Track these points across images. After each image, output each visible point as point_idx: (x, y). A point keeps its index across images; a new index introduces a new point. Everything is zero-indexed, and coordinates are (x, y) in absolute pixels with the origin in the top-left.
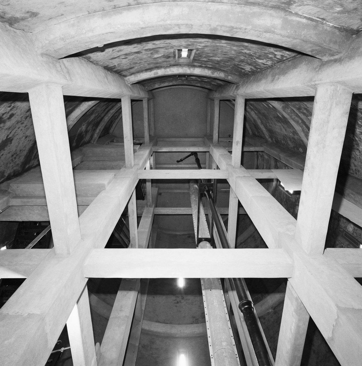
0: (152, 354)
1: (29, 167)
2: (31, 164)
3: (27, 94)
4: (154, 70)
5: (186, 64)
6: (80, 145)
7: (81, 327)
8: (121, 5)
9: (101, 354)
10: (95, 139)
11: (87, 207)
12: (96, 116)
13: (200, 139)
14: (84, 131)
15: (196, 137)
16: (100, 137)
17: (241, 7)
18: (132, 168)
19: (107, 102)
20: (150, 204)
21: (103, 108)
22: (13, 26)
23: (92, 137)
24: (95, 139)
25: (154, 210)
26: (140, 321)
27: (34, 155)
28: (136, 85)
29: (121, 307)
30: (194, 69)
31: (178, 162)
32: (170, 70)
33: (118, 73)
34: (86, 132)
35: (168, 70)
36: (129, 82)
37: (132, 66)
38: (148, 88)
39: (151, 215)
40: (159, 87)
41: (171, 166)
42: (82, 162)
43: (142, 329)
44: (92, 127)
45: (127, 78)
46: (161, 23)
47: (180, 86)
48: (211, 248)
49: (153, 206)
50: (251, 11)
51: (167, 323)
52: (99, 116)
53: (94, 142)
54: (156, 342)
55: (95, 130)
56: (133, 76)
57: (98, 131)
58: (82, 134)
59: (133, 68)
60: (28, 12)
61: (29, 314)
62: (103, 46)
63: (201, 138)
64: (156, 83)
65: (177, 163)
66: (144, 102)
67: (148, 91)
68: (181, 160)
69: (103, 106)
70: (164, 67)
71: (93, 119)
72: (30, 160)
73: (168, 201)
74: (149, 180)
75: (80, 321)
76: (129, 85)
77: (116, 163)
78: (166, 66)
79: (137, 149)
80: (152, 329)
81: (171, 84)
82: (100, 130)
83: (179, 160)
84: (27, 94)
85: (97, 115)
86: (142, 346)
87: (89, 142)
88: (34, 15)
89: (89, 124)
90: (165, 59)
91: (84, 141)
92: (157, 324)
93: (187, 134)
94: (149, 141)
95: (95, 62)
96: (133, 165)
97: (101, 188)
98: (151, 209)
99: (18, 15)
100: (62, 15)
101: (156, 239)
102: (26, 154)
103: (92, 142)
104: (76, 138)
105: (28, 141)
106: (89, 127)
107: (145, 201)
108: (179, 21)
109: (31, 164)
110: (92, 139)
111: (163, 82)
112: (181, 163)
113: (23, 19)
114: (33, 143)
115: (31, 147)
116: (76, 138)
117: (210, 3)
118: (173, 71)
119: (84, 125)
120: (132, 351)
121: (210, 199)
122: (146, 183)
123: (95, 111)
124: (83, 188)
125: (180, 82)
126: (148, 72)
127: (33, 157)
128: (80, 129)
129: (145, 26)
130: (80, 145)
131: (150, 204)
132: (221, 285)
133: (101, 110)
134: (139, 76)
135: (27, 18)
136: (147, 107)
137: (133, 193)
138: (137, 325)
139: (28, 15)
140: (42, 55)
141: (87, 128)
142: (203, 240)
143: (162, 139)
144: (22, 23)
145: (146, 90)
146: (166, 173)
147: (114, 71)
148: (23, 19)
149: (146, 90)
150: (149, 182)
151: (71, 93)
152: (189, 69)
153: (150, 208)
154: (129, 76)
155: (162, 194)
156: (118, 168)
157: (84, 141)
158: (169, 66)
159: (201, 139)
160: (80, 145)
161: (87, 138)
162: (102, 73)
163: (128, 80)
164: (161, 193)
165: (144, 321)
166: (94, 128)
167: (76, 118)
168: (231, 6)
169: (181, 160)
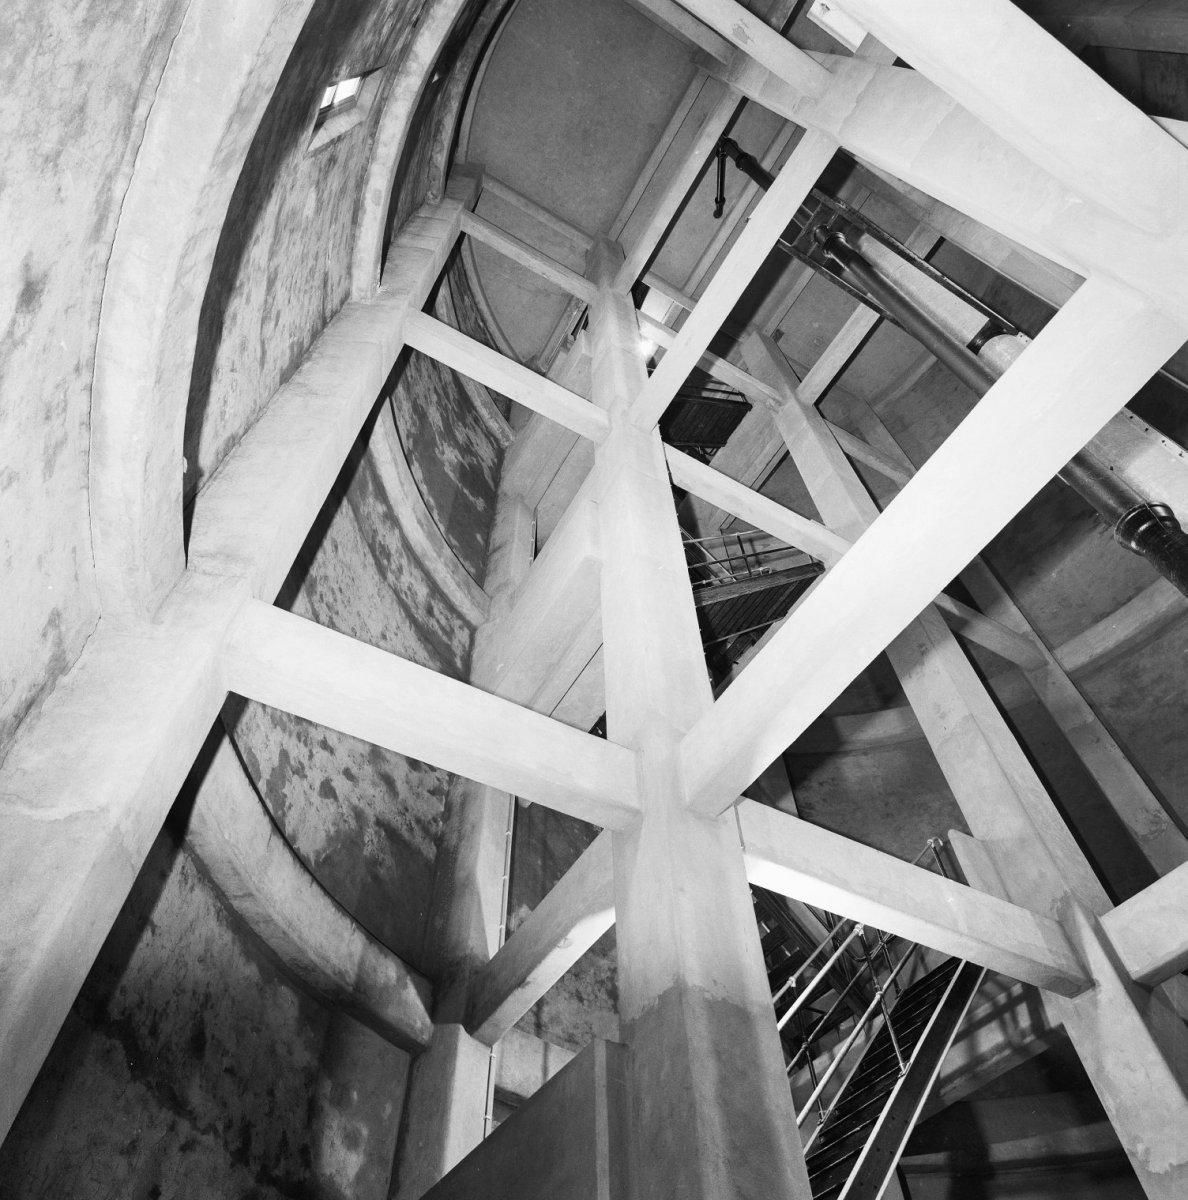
0: (1157, 700)
1: (462, 658)
2: (459, 651)
3: (232, 696)
4: (364, 198)
5: (388, 80)
6: (491, 484)
7: (831, 882)
8: (86, 409)
9: (982, 842)
10: (503, 432)
11: (601, 662)
12: (439, 403)
13: (695, 85)
14: (461, 459)
15: (683, 94)
16: (507, 419)
17: (175, 62)
18: (611, 429)
19: (388, 399)
20: (774, 399)
21: (423, 369)
22: (70, 665)
23: (489, 435)
24: (503, 432)
25: (798, 401)
26: (1046, 663)
27: (440, 632)
28: (393, 252)
29: (937, 707)
30: (416, 55)
31: (718, 213)
32: (386, 145)
33: (325, 324)
34: (467, 449)
35: (381, 151)
36: (369, 294)
37: (317, 282)
38: (435, 192)
39: (805, 423)
40: (445, 153)
41: (717, 246)
42: (535, 514)
43: (1069, 674)
44: (465, 425)
45: (355, 295)
46: (157, 332)
47: (483, 66)
48: (1021, 348)
49: (788, 392)
50: (197, 31)
51: (1130, 599)
52: (440, 391)
53: (508, 440)
54: (1141, 666)
55: (477, 419)
56: (355, 272)
57: (484, 412)
58: (464, 467)
59: (326, 274)
60: (44, 635)
61: (660, 997)
62: (186, 460)
63: (692, 79)
64: (431, 157)
65: (721, 220)
66: (468, 231)
67: (443, 198)
68: (720, 201)
69: (418, 370)
70: (368, 160)
71: (441, 415)
72: (448, 648)
73: (816, 325)
74: (703, 359)
75: (816, 876)
76: (379, 290)
77: (576, 458)
78: (367, 153)
79: (584, 351)
80: (1099, 650)
81: (455, 105)
82: (485, 404)
83: (714, 207)
84: (232, 696)
85: (434, 398)
86: (1112, 706)
87: (500, 453)
88: (55, 619)
89: (449, 434)
90: (336, 168)
91: (490, 468)
92: (1101, 626)
93: (652, 126)
94: (591, 287)
95: (252, 419)
96: (606, 422)
97: (592, 570)
98: (792, 406)
99: (46, 655)
100: (74, 550)
101: (891, 440)
102: (428, 652)
103: (506, 444)
104: (466, 491)
105: (396, 635)
106: (457, 434)
107: (757, 408)
108: (166, 280)
109: (459, 651)
110: (496, 440)
111: (438, 131)
112: (726, 209)
113: (59, 642)
114: (408, 624)
115: (415, 632)
116: (466, 491)
117: (138, 163)
118: (394, 135)
119: (443, 453)
120: (1092, 741)
121: (853, 266)
122: (710, 376)
123: (421, 401)
124: (566, 609)
125: (463, 66)
126: (362, 219)
127: (445, 638)
128: (447, 469)
129: (154, 376)
130: (491, 484)
131: (774, 399)
132: (1136, 418)
133: (430, 377)
134: (362, 255)
135: (60, 632)
136: (486, 232)
137: (670, 474)
138: (1046, 679)
139: (51, 637)
140: (155, 620)
141: (456, 444)
142: (979, 342)
143: (619, 225)
144: (68, 643)
145: (438, 200)
146: (687, 344)
147: (311, 343)
148: (59, 642)
149: (438, 200)
150: (711, 364)
151: (383, 368)
152: (408, 74)
153: (787, 406)
154: (350, 283)
155: (783, 329)
156: (587, 466)
157: (490, 468)
158: (370, 141)
159: (694, 82)
160: (493, 487)
161: (486, 452)
162: (291, 402)
163: (363, 294)
164: (778, 330)
165: (1058, 652)
166: (469, 419)
167: (402, 484)
168: (162, 96)
169: (720, 201)
